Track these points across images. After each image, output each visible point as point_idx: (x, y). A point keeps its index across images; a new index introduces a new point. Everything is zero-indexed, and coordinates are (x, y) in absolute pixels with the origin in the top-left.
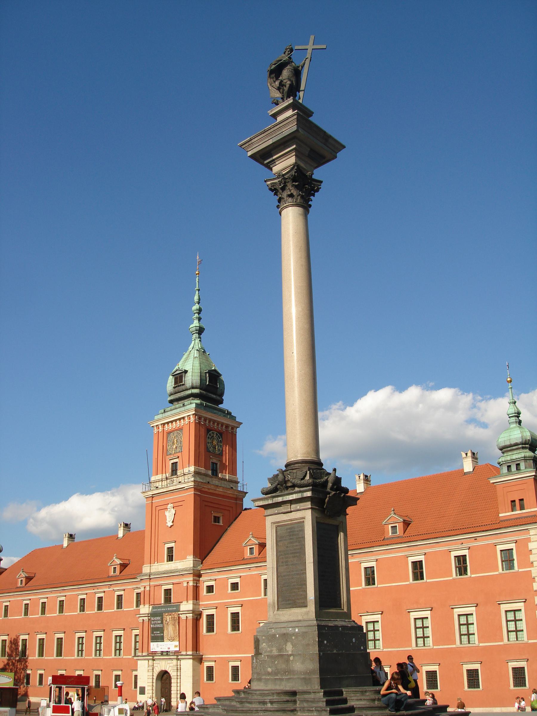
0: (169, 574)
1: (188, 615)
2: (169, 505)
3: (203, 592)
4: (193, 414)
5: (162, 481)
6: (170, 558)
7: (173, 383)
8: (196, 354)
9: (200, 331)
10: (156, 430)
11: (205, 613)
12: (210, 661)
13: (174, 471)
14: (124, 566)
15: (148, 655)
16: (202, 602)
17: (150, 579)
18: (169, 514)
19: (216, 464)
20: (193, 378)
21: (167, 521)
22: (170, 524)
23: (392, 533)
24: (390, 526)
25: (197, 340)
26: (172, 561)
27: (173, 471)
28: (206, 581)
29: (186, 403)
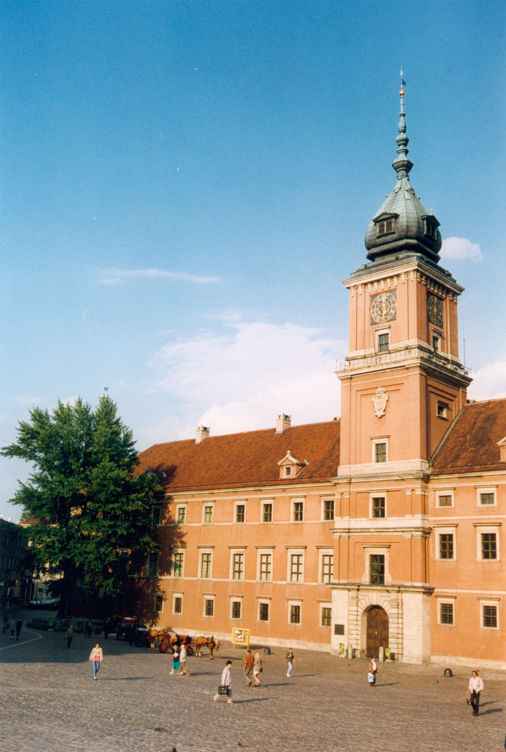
1: (414, 533)
2: (380, 389)
4: (414, 270)
8: (407, 196)
11: (438, 532)
17: (350, 483)
21: (376, 410)
26: (384, 460)
27: (380, 345)
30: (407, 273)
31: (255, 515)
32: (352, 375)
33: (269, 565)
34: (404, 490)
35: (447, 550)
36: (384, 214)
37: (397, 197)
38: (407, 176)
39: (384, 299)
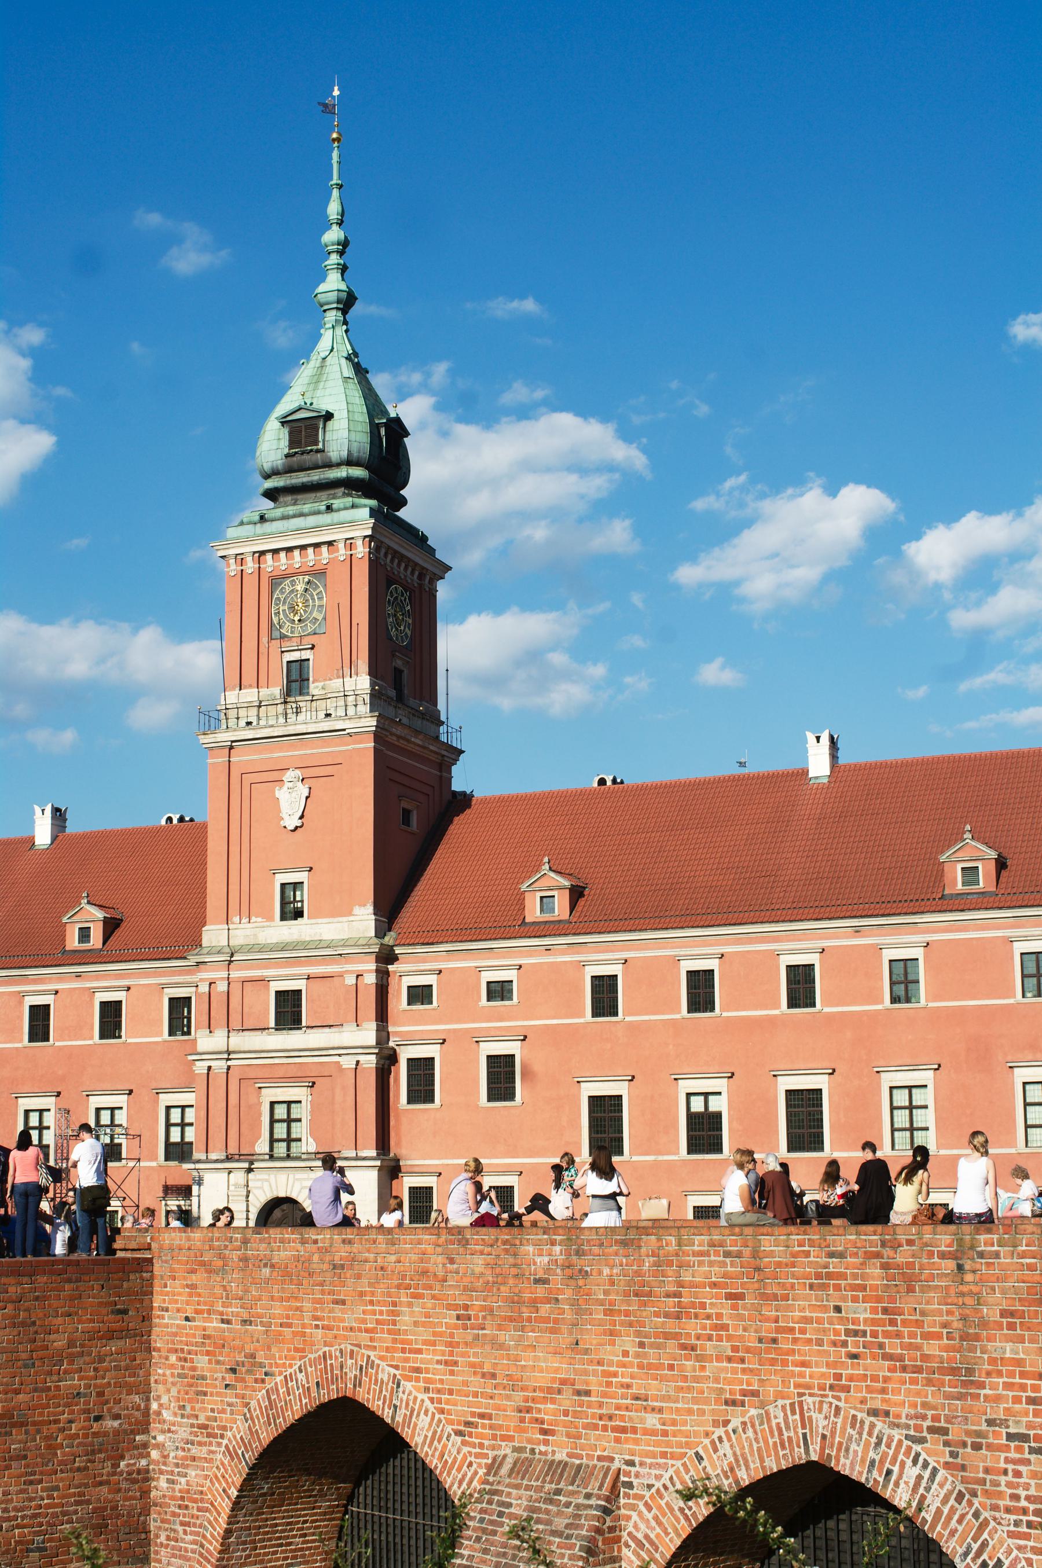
0: (290, 953)
1: (361, 1058)
3: (399, 1001)
4: (365, 537)
5: (260, 706)
6: (292, 912)
7: (287, 443)
9: (347, 303)
10: (233, 568)
12: (422, 1174)
13: (297, 679)
14: (111, 926)
15: (229, 1159)
16: (395, 1025)
18: (290, 800)
19: (401, 672)
20: (353, 437)
21: (284, 815)
22: (292, 822)
23: (964, 884)
24: (960, 866)
25: (341, 330)
28: (408, 972)
29: (337, 503)
30: (349, 542)
31: (75, 1034)
32: (232, 742)
33: (45, 1132)
34: (341, 975)
35: (422, 1086)
36: (300, 409)
37: (327, 370)
38: (345, 323)
39: (300, 587)
